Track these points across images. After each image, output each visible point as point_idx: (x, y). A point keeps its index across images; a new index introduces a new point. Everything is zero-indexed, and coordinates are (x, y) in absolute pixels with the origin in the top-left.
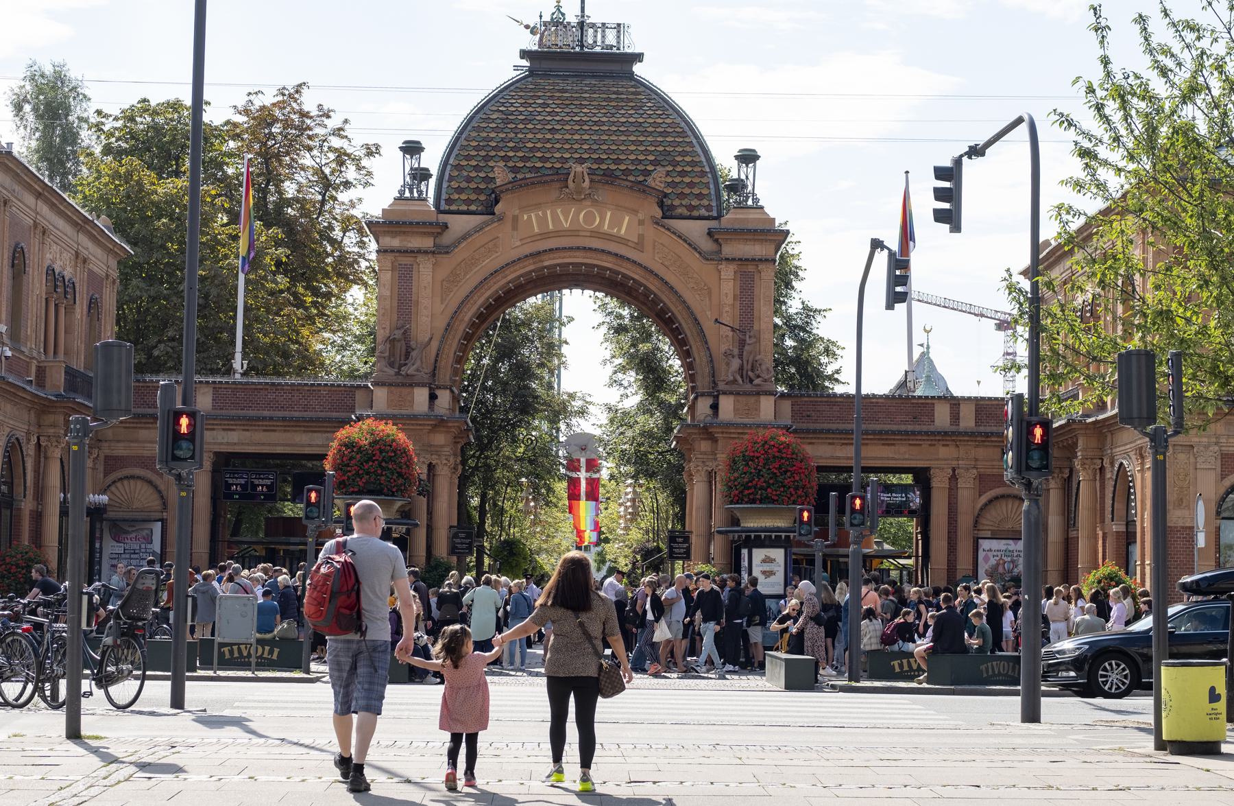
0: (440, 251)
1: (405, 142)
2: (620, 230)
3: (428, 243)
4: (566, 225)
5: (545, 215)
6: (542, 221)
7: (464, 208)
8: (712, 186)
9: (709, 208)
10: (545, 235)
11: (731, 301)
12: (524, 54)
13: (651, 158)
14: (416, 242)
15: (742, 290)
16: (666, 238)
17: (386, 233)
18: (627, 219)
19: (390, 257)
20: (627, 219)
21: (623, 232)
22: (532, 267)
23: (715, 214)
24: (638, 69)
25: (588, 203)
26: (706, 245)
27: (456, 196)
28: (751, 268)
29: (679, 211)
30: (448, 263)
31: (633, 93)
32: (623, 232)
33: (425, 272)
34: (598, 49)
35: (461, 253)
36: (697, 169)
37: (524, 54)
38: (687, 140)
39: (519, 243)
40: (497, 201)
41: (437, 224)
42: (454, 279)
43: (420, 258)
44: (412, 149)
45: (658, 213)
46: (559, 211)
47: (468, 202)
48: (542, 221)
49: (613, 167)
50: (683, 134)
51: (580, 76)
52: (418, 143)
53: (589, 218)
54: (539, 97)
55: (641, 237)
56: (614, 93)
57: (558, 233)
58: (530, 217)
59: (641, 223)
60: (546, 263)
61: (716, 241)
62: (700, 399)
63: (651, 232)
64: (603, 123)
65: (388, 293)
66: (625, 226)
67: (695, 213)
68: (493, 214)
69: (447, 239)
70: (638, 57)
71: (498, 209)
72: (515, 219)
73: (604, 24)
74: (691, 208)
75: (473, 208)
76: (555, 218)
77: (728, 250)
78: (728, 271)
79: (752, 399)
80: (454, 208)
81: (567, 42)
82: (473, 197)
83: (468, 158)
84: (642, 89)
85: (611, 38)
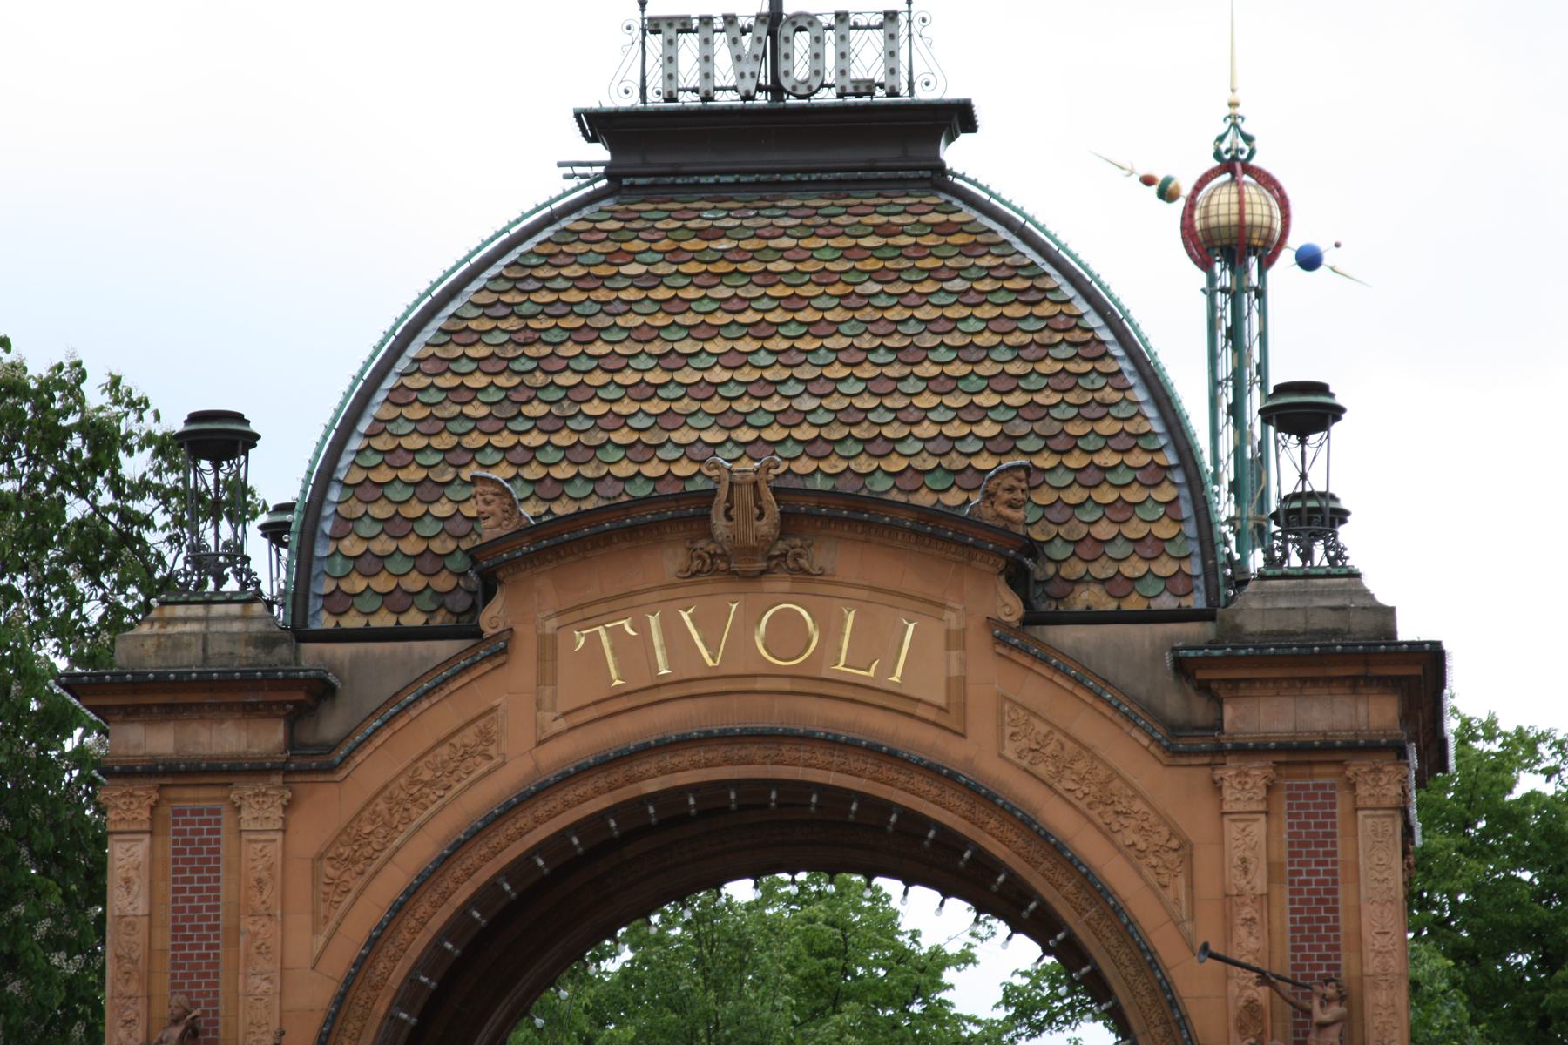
0: (307, 764)
1: (194, 418)
3: (268, 738)
5: (642, 627)
7: (385, 620)
8: (1186, 510)
9: (1177, 582)
10: (652, 693)
11: (1260, 883)
12: (596, 124)
13: (988, 429)
14: (226, 739)
15: (1297, 848)
16: (1035, 689)
22: (603, 802)
23: (1197, 601)
24: (957, 155)
25: (779, 584)
26: (1175, 702)
27: (359, 584)
28: (1324, 776)
29: (1088, 598)
30: (329, 807)
31: (935, 229)
33: (265, 839)
34: (827, 97)
35: (375, 769)
36: (1138, 459)
37: (596, 124)
38: (1107, 366)
39: (562, 724)
40: (488, 594)
41: (290, 682)
42: (351, 852)
43: (244, 790)
45: (1010, 607)
47: (397, 600)
48: (634, 651)
49: (864, 465)
50: (1091, 350)
51: (772, 186)
52: (238, 417)
53: (787, 634)
54: (633, 257)
55: (956, 686)
56: (877, 230)
58: (594, 640)
59: (955, 640)
60: (651, 786)
61: (1204, 688)
63: (992, 677)
64: (835, 328)
65: (142, 907)
67: (1134, 603)
68: (477, 634)
69: (331, 726)
71: (492, 618)
72: (548, 649)
73: (841, 17)
74: (1118, 585)
75: (414, 619)
76: (674, 632)
78: (1244, 785)
80: (352, 621)
81: (724, 76)
82: (414, 582)
83: (396, 457)
84: (968, 213)
85: (867, 61)
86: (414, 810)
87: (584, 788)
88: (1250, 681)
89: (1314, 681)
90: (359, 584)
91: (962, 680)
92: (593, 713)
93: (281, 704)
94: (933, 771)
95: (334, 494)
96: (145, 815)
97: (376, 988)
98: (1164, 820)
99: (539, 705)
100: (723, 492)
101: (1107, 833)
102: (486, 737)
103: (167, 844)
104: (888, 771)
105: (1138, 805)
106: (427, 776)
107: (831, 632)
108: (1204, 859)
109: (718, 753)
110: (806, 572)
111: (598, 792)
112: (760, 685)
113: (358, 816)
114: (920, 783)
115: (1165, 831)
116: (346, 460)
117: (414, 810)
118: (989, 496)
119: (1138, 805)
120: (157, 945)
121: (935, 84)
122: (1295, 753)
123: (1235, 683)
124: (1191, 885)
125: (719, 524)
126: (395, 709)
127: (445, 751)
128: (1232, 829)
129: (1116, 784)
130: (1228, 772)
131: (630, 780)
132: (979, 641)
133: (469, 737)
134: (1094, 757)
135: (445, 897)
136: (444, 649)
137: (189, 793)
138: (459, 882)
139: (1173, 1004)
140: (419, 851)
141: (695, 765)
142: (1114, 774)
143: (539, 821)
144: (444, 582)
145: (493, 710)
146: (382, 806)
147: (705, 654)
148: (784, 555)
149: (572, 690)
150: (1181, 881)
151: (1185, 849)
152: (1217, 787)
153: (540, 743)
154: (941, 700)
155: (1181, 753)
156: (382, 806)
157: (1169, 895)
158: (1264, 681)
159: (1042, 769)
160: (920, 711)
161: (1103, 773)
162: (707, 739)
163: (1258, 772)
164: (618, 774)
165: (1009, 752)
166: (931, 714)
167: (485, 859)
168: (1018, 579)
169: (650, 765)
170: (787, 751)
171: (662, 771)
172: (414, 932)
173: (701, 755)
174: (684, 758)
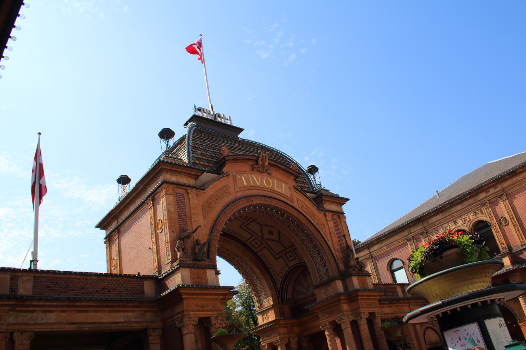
2: (282, 190)
5: (248, 177)
6: (247, 180)
9: (308, 188)
25: (265, 174)
27: (198, 162)
33: (195, 200)
35: (210, 191)
44: (166, 134)
55: (291, 195)
57: (256, 188)
58: (241, 177)
59: (290, 189)
71: (225, 169)
72: (234, 178)
79: (363, 278)
89: (335, 202)
90: (198, 162)
95: (190, 147)
108: (326, 226)
110: (269, 173)
122: (334, 212)
125: (260, 162)
126: (212, 181)
132: (292, 189)
136: (214, 176)
137: (179, 189)
140: (219, 207)
145: (227, 185)
151: (324, 225)
152: (325, 215)
153: (236, 192)
155: (321, 210)
163: (330, 214)
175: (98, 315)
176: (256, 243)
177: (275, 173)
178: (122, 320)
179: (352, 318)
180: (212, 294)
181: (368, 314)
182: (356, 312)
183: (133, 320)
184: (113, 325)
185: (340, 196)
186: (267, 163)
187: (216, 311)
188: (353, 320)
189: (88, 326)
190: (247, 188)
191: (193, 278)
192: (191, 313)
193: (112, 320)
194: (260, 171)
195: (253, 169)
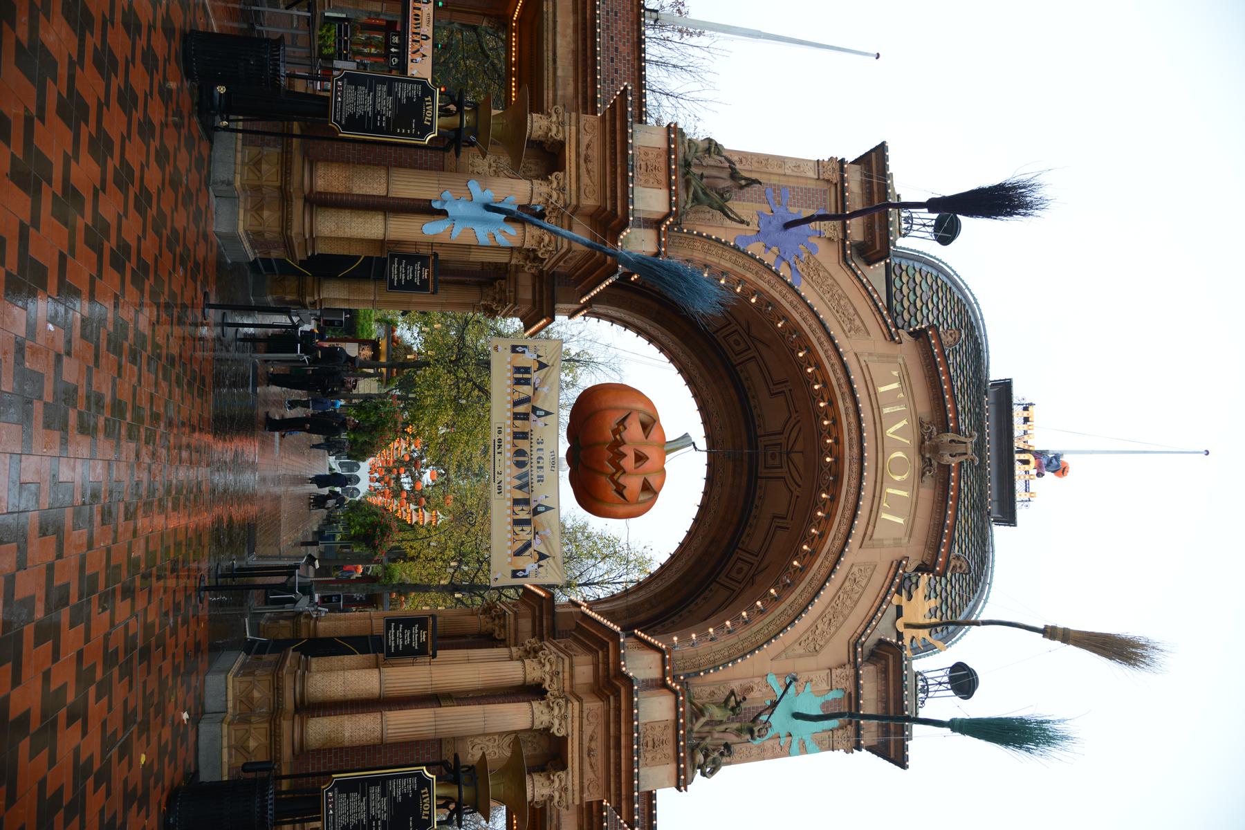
2: (888, 512)
4: (890, 432)
5: (899, 402)
10: (876, 408)
12: (1005, 388)
17: (868, 174)
18: (900, 521)
19: (835, 178)
20: (900, 521)
21: (885, 516)
26: (870, 642)
32: (885, 516)
35: (843, 278)
39: (863, 364)
40: (910, 334)
46: (905, 422)
53: (899, 466)
57: (878, 421)
59: (897, 542)
62: (658, 656)
63: (882, 559)
66: (893, 519)
70: (1009, 518)
72: (889, 358)
77: (869, 674)
79: (669, 749)
86: (828, 296)
87: (840, 374)
88: (886, 679)
90: (905, 279)
91: (883, 546)
92: (868, 378)
93: (873, 240)
94: (848, 535)
95: (935, 273)
96: (826, 177)
97: (757, 273)
98: (827, 642)
99: (870, 354)
100: (962, 439)
101: (822, 616)
102: (857, 330)
103: (812, 185)
104: (848, 514)
105: (833, 629)
106: (842, 303)
107: (899, 485)
108: (810, 662)
109: (854, 435)
110: (923, 474)
111: (838, 380)
112: (880, 455)
113: (826, 271)
114: (844, 528)
115: (822, 643)
116: (945, 279)
117: (828, 296)
118: (958, 557)
119: (833, 629)
120: (772, 177)
121: (1021, 512)
123: (885, 671)
124: (800, 656)
125: (947, 437)
127: (852, 311)
128: (824, 673)
129: (841, 619)
130: (849, 671)
131: (843, 394)
132: (897, 554)
133: (858, 322)
134: (852, 608)
135: (795, 307)
138: (801, 314)
139: (752, 652)
141: (849, 424)
142: (846, 618)
143: (826, 352)
144: (906, 316)
146: (830, 281)
147: (892, 430)
148: (931, 465)
149: (876, 369)
150: (801, 651)
152: (842, 666)
154: (875, 537)
156: (830, 281)
157: (796, 646)
158: (887, 685)
159: (847, 584)
160: (870, 527)
161: (846, 612)
162: (860, 430)
163: (849, 685)
164: (845, 389)
165: (855, 569)
166: (869, 532)
167: (810, 326)
168: (922, 568)
169: (849, 404)
170: (855, 467)
171: (846, 409)
172: (780, 292)
173: (854, 426)
174: (852, 419)
175: (570, 31)
176: (740, 571)
177: (927, 493)
178: (559, 73)
179: (552, 687)
180: (614, 173)
181: (563, 733)
182: (572, 694)
183: (560, 93)
184: (550, 54)
185: (909, 743)
186: (947, 459)
187: (578, 188)
188: (546, 692)
189: (551, 10)
190: (872, 392)
191: (646, 154)
192: (573, 128)
193: (559, 51)
194: (923, 442)
195: (921, 424)
